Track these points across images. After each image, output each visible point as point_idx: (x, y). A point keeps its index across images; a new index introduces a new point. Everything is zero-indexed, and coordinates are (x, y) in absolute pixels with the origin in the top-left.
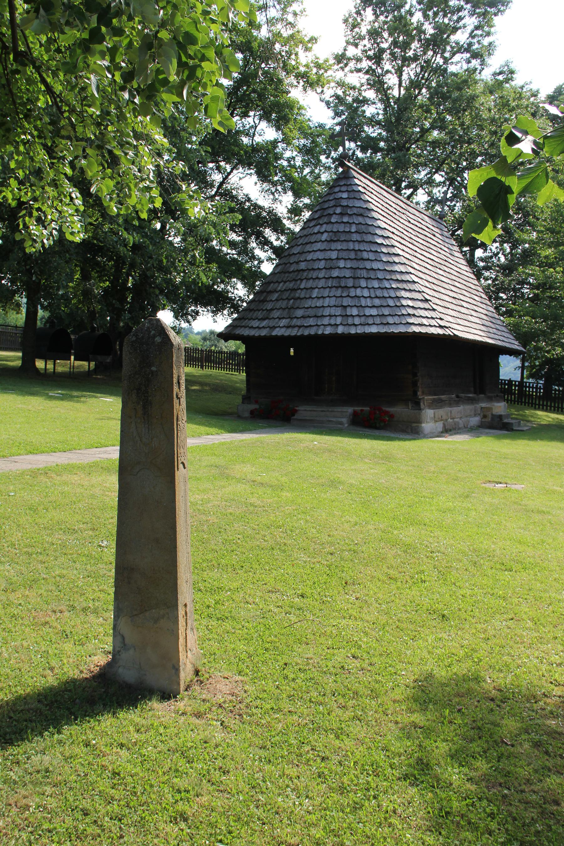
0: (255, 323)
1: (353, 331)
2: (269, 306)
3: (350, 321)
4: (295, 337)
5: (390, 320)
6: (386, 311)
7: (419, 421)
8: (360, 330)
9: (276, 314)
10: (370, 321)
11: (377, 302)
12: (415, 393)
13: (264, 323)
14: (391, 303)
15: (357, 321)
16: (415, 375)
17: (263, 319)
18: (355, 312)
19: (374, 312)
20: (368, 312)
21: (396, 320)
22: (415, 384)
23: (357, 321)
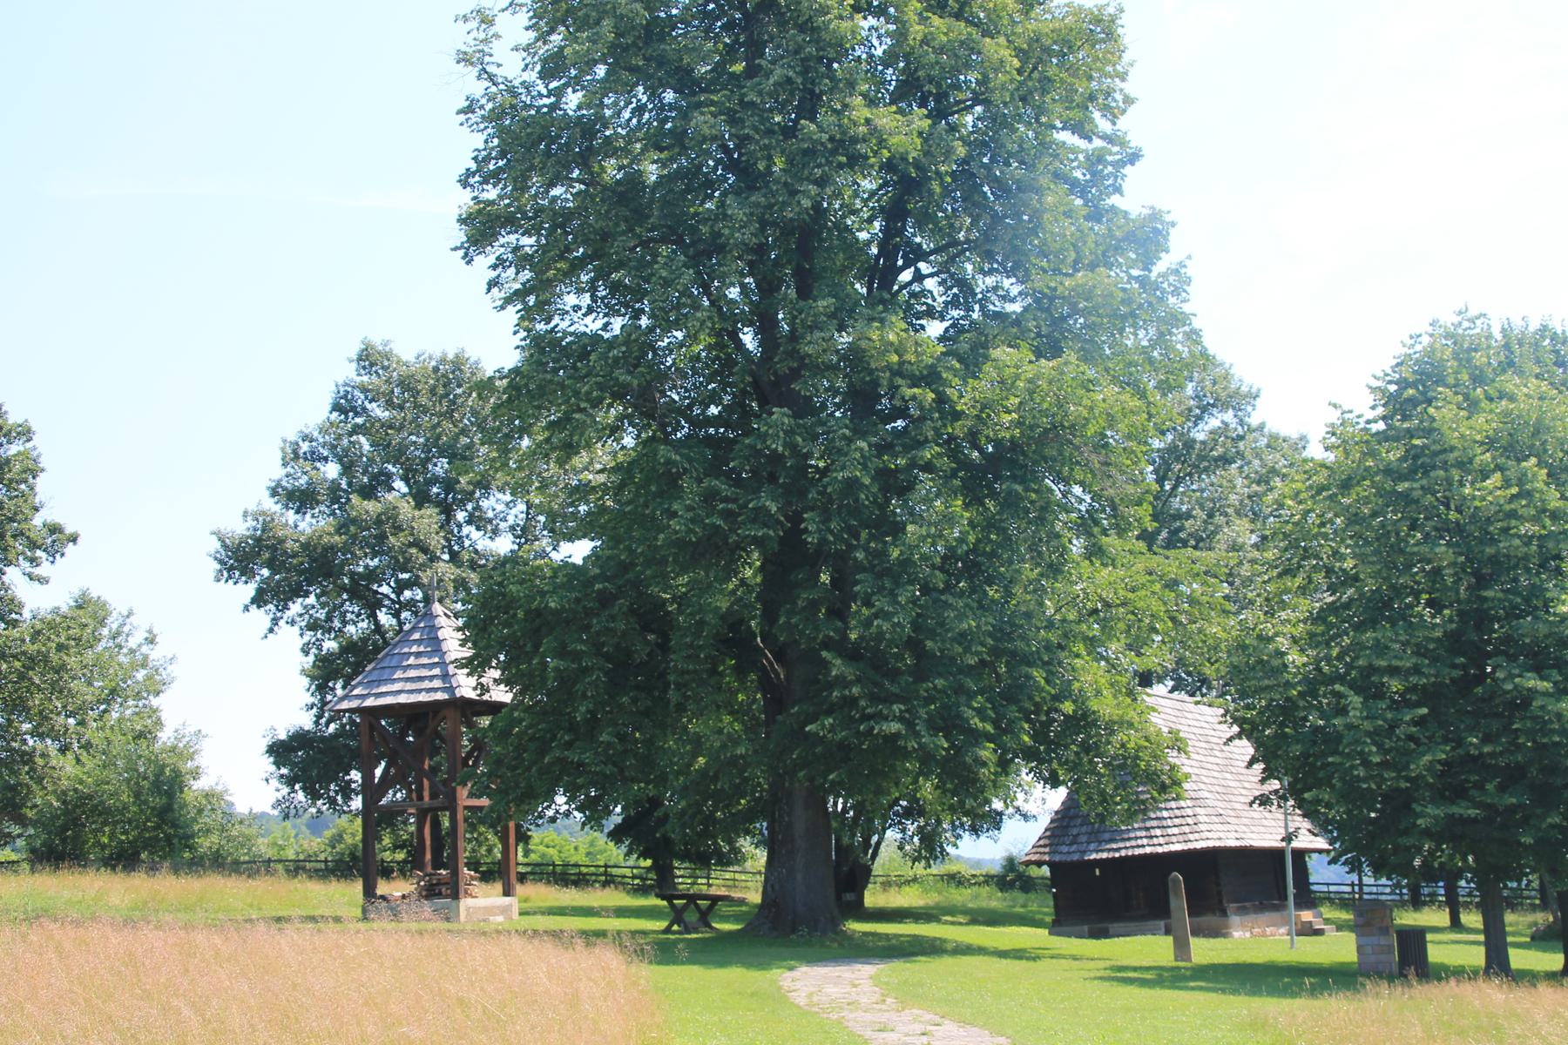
0: (1065, 849)
1: (1160, 850)
2: (1075, 832)
3: (1155, 841)
4: (1102, 860)
5: (1191, 837)
6: (1187, 829)
7: (1227, 927)
8: (1166, 849)
9: (1084, 838)
10: (1174, 839)
11: (1177, 821)
12: (1221, 902)
13: (1074, 848)
14: (1190, 821)
15: (1161, 840)
16: (1218, 885)
17: (1071, 844)
18: (1158, 832)
19: (1175, 831)
20: (1170, 831)
21: (1197, 836)
22: (1219, 893)
23: (1161, 840)
